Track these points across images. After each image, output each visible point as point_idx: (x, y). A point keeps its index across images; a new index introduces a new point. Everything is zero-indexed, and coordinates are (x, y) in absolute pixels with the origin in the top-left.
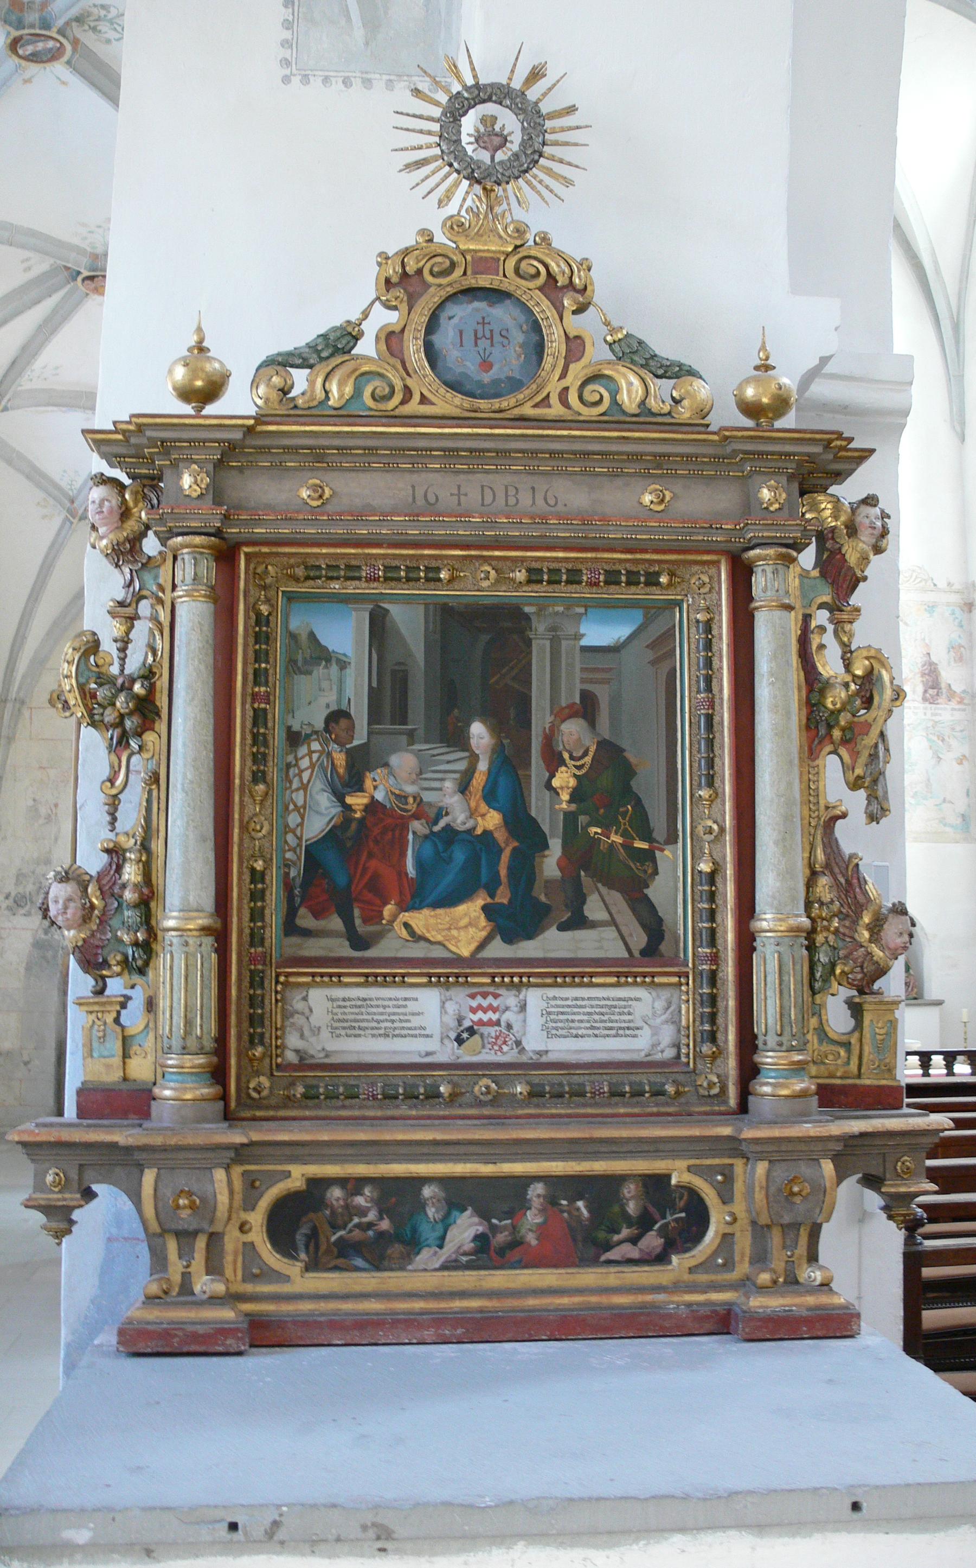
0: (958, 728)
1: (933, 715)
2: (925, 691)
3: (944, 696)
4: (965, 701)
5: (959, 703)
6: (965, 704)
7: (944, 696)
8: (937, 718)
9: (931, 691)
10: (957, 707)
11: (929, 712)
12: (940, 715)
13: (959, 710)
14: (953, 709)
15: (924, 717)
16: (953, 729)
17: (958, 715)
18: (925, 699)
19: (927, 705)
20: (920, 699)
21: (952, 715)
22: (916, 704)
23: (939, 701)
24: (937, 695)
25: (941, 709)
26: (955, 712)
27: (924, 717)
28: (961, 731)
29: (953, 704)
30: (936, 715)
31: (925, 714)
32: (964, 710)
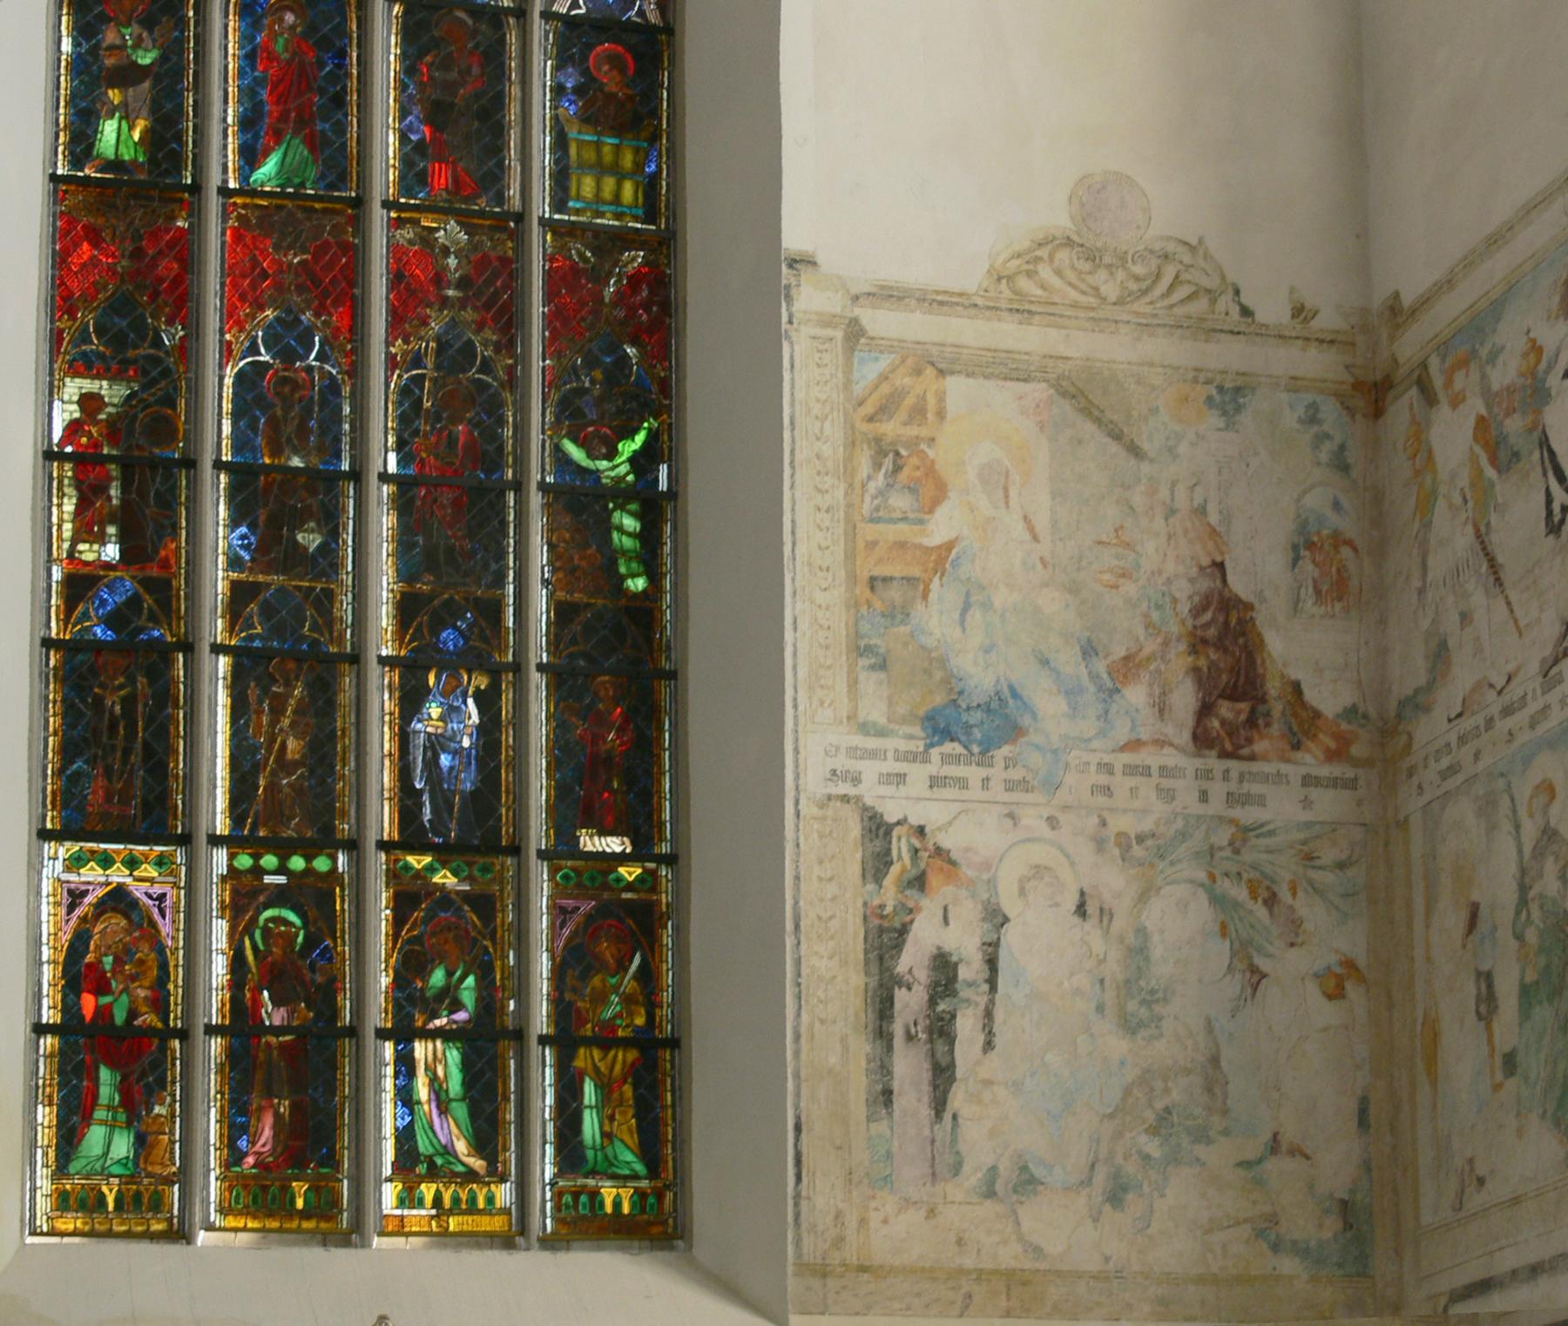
0: (1328, 855)
1: (1231, 799)
2: (1205, 710)
3: (1276, 729)
4: (1356, 750)
5: (1332, 756)
6: (1356, 763)
7: (1276, 729)
8: (1249, 815)
9: (1225, 709)
10: (1325, 771)
11: (1218, 790)
12: (1261, 801)
13: (1334, 783)
14: (1308, 781)
15: (1197, 809)
16: (1309, 857)
17: (1329, 804)
18: (1202, 740)
19: (1212, 762)
20: (1185, 737)
21: (1307, 803)
22: (1170, 758)
23: (1260, 746)
24: (1251, 722)
25: (1266, 778)
26: (1314, 793)
27: (1197, 809)
28: (1342, 866)
29: (1310, 761)
30: (1246, 800)
31: (1204, 797)
32: (1351, 784)
